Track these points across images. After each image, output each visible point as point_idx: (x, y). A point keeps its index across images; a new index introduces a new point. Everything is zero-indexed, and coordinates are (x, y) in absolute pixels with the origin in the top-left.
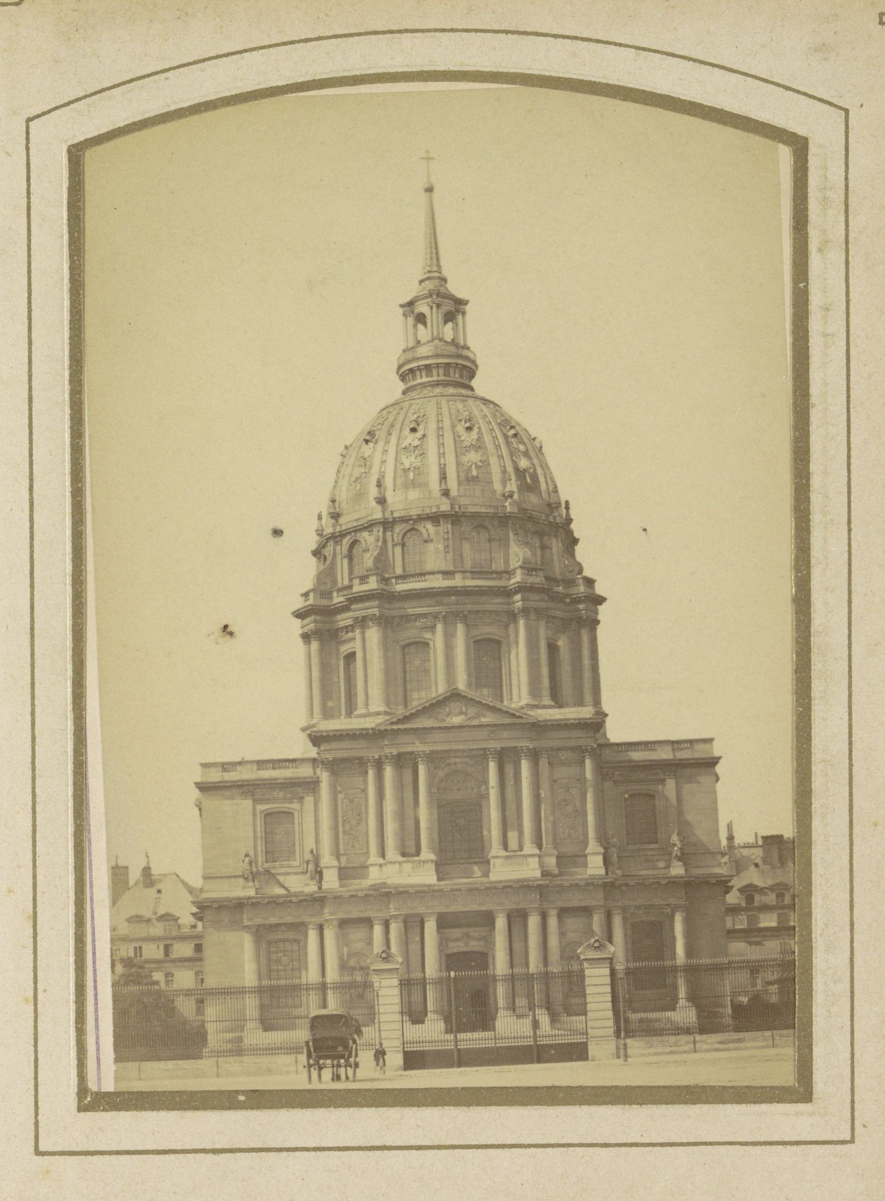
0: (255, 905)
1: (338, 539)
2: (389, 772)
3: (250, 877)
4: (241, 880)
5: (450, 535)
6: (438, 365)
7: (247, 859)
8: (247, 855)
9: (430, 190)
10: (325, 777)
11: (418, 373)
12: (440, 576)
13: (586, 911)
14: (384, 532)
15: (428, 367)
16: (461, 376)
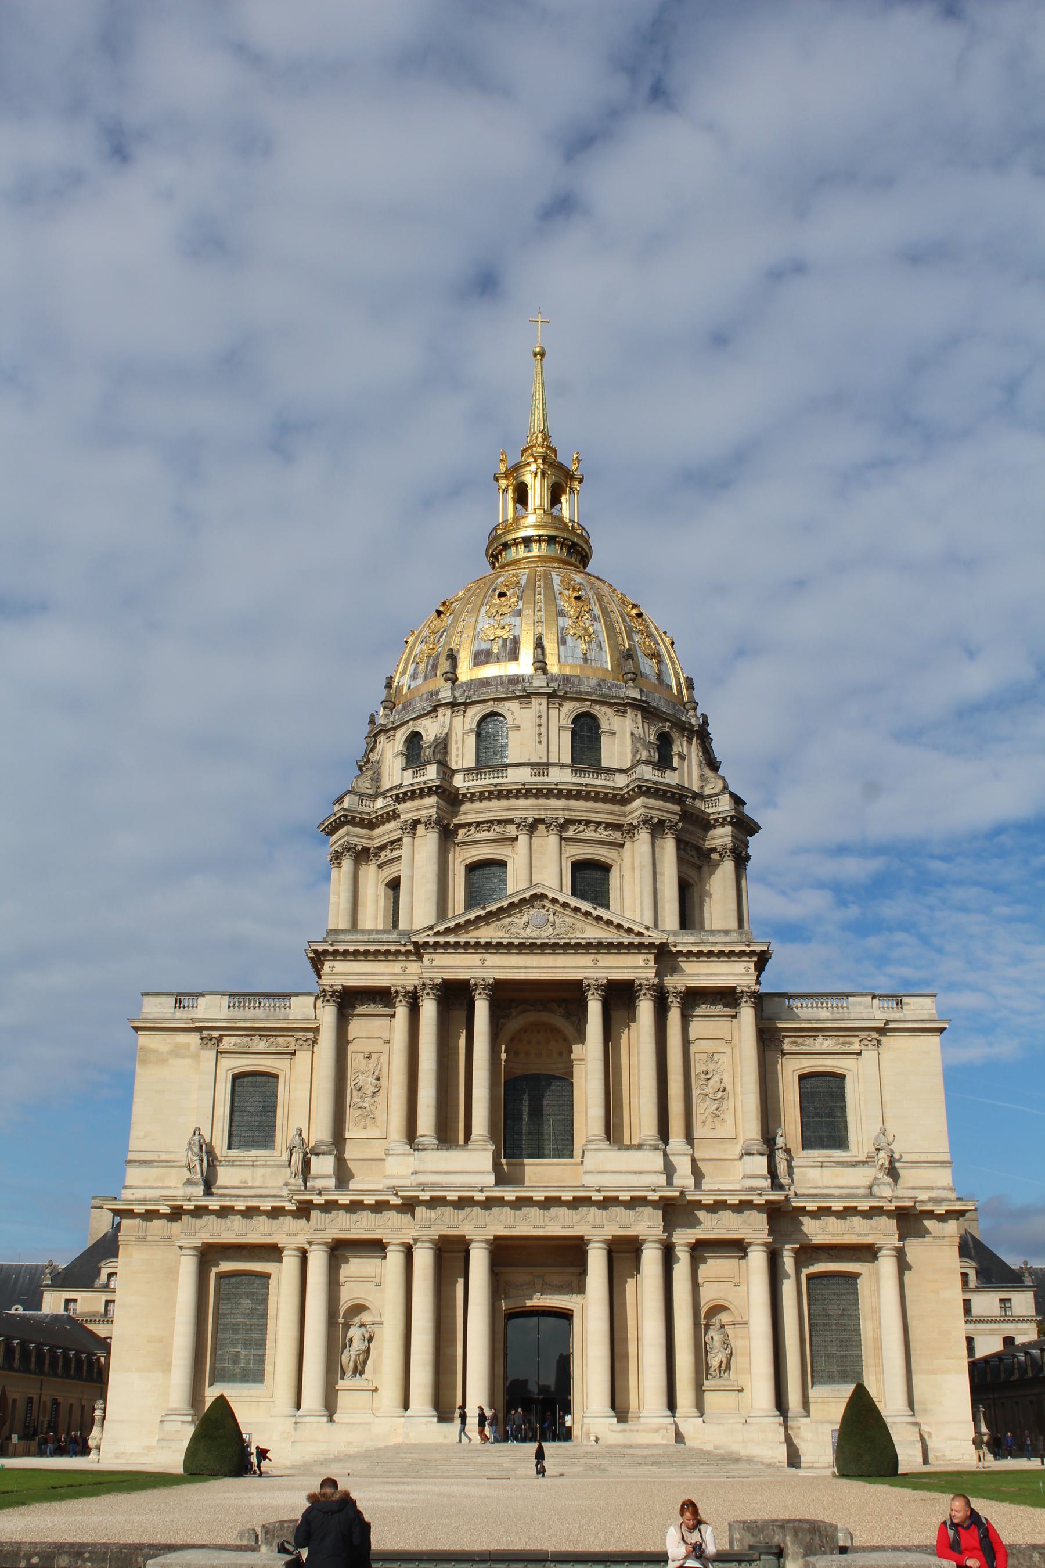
0: (199, 1212)
1: (391, 733)
2: (429, 1009)
3: (198, 1167)
4: (185, 1171)
5: (544, 720)
6: (540, 539)
7: (197, 1137)
8: (197, 1131)
9: (542, 354)
10: (328, 1015)
11: (514, 549)
12: (527, 770)
13: (738, 1247)
14: (452, 717)
15: (527, 541)
16: (569, 553)
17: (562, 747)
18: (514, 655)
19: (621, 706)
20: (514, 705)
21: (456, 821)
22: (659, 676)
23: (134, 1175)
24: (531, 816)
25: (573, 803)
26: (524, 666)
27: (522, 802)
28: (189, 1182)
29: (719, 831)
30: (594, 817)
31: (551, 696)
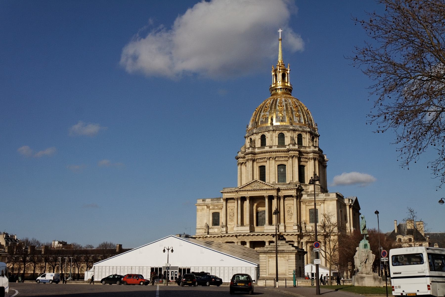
15: (276, 89)
17: (276, 141)
18: (268, 122)
19: (289, 130)
20: (267, 133)
21: (256, 158)
22: (299, 121)
23: (198, 231)
24: (269, 157)
25: (278, 153)
26: (269, 124)
27: (267, 154)
28: (205, 232)
29: (311, 154)
30: (281, 156)
31: (273, 131)
